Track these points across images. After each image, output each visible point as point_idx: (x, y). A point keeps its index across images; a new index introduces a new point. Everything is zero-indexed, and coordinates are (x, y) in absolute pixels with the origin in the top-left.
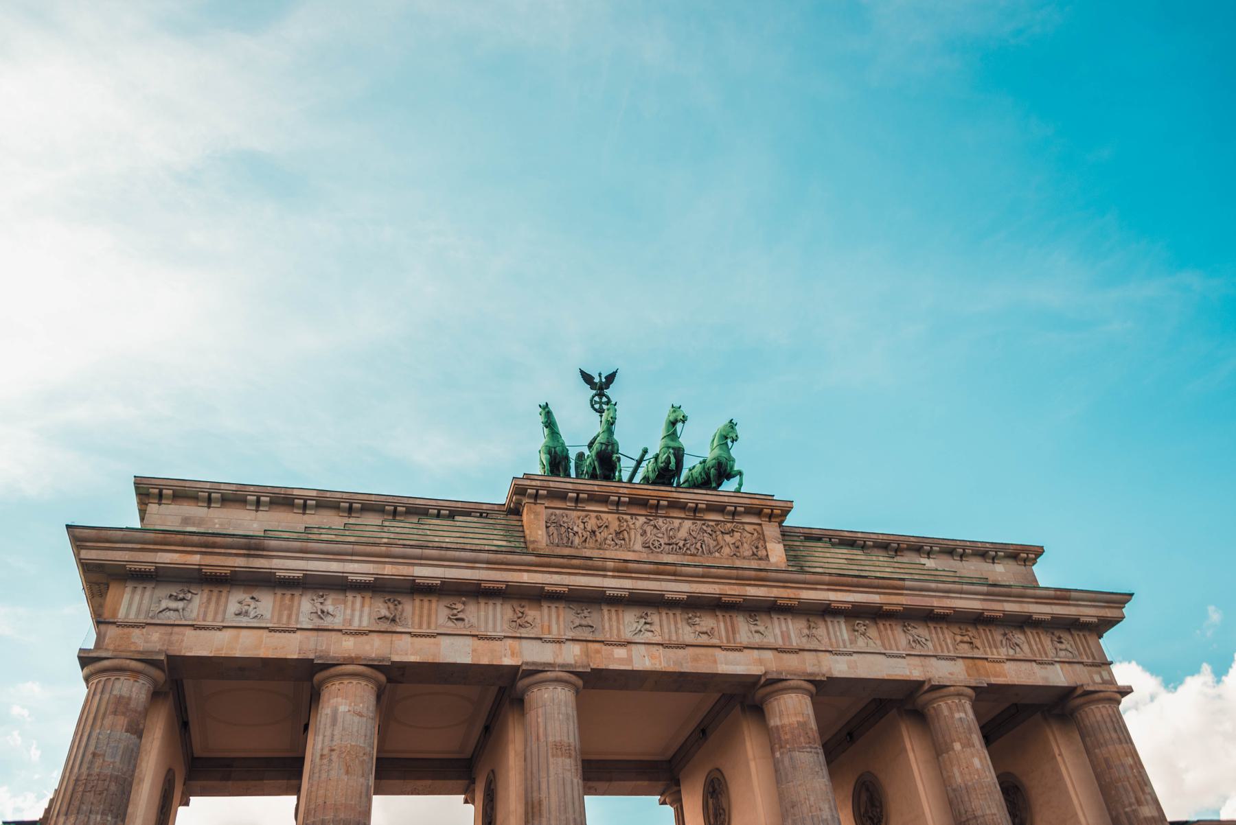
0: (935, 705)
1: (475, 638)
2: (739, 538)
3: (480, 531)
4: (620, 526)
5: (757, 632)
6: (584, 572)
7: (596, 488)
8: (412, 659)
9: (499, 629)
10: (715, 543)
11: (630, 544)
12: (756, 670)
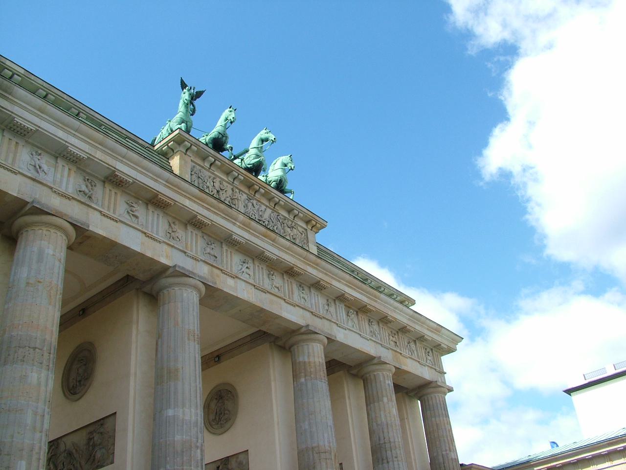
0: (375, 373)
1: (143, 235)
5: (303, 298)
6: (224, 216)
8: (101, 232)
9: (160, 235)
12: (301, 322)
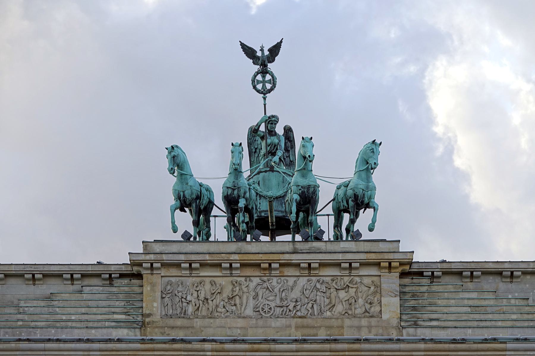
2: (353, 294)
3: (104, 303)
4: (233, 291)
7: (207, 257)
10: (327, 301)
11: (241, 308)
